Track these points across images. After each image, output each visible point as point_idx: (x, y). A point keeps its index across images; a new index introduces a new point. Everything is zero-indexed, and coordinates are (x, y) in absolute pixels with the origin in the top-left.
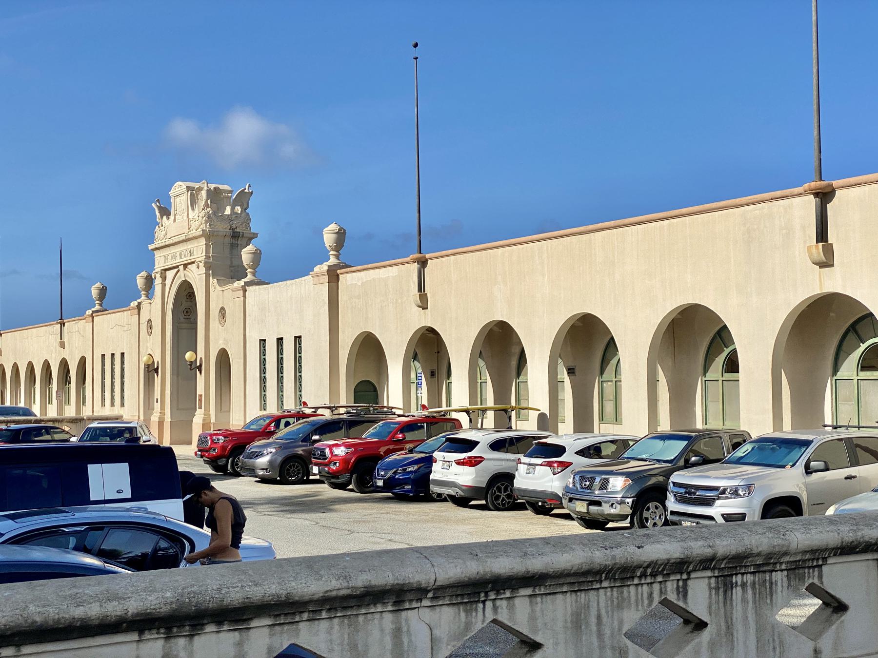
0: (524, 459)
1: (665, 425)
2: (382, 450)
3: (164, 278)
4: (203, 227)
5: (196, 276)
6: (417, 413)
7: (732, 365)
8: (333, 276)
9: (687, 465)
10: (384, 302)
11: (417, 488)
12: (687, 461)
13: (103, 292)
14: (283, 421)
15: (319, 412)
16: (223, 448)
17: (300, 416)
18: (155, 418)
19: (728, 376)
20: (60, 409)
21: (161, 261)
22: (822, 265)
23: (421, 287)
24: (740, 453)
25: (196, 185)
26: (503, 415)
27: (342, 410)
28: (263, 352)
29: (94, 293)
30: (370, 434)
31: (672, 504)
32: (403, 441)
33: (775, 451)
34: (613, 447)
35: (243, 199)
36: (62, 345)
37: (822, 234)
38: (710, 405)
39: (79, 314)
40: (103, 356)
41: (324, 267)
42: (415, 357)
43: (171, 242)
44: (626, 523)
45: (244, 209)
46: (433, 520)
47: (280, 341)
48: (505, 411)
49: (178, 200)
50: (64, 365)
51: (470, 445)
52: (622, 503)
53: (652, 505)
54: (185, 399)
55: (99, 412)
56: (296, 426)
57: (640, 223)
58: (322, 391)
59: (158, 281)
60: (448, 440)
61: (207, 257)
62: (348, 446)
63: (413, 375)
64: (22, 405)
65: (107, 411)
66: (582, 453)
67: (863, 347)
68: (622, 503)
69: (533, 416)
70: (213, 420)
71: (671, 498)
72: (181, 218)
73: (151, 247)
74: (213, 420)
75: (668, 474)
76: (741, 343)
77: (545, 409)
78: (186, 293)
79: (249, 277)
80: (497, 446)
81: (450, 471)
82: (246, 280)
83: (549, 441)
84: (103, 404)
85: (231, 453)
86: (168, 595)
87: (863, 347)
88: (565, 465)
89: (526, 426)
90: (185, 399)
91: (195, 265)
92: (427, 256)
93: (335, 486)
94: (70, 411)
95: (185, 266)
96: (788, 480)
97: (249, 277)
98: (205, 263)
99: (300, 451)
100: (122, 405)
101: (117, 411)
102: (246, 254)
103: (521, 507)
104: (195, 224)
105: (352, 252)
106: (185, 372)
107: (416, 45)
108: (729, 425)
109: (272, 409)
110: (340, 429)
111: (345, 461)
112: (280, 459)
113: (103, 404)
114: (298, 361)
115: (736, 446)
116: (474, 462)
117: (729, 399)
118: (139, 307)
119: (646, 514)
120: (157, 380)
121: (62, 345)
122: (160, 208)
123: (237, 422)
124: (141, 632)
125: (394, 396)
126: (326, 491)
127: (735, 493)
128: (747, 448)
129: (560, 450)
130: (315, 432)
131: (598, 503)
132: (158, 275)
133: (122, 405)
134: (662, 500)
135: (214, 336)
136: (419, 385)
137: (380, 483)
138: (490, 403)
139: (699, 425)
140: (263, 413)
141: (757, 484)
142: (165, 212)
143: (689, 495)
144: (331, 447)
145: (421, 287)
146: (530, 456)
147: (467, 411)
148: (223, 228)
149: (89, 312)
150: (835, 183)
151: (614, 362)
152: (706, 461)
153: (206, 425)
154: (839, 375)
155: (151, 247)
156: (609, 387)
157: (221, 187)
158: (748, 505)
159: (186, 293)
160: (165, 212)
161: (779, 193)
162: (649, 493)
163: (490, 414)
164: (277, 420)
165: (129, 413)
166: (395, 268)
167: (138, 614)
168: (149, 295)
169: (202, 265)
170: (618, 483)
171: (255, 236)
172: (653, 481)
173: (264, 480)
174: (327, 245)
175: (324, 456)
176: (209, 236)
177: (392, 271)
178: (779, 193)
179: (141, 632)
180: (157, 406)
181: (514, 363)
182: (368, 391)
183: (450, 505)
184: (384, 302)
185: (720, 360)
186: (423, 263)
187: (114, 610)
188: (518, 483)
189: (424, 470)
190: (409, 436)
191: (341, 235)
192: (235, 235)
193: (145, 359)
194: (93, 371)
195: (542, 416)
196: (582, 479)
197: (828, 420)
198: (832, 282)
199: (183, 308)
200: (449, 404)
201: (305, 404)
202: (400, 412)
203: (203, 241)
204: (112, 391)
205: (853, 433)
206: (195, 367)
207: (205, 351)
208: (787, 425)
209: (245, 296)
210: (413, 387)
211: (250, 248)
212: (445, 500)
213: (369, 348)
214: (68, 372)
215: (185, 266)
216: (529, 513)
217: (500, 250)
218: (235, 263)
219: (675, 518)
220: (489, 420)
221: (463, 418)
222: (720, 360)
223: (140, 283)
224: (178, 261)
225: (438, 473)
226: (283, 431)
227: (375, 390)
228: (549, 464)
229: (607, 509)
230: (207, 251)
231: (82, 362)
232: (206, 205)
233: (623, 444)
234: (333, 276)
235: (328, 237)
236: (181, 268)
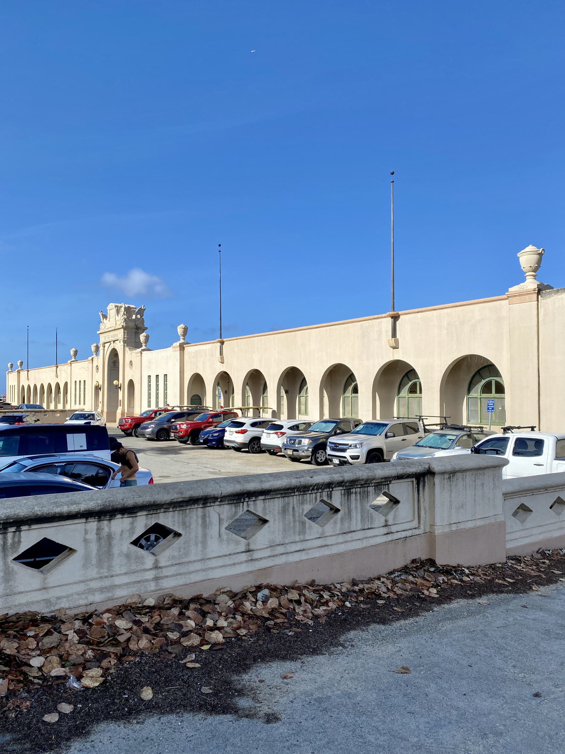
0: (265, 431)
1: (326, 417)
2: (203, 426)
3: (104, 347)
4: (122, 324)
5: (119, 346)
6: (219, 410)
8: (182, 348)
9: (336, 434)
10: (205, 359)
11: (218, 443)
12: (335, 432)
13: (76, 353)
14: (158, 413)
15: (175, 409)
16: (130, 425)
17: (166, 410)
18: (99, 410)
19: (354, 395)
20: (56, 406)
21: (102, 339)
22: (394, 348)
23: (221, 354)
24: (358, 429)
25: (119, 305)
26: (257, 411)
27: (185, 408)
28: (149, 381)
29: (72, 353)
30: (197, 419)
31: (329, 451)
32: (210, 422)
33: (372, 428)
34: (304, 426)
35: (141, 312)
36: (57, 376)
37: (394, 335)
38: (346, 407)
39: (64, 362)
40: (76, 382)
41: (178, 344)
42: (218, 385)
43: (107, 330)
44: (309, 459)
45: (141, 316)
46: (225, 458)
47: (157, 376)
48: (258, 409)
49: (111, 311)
50: (58, 385)
51: (241, 424)
52: (307, 450)
53: (320, 451)
54: (113, 402)
55: (73, 408)
56: (164, 414)
57: (317, 328)
58: (175, 400)
59: (101, 348)
60: (232, 422)
61: (124, 338)
62: (187, 424)
63: (217, 393)
64: (38, 403)
65: (77, 407)
66: (290, 428)
67: (410, 383)
68: (307, 450)
69: (270, 411)
70: (126, 412)
71: (328, 448)
72: (112, 320)
73: (98, 332)
74: (126, 412)
75: (327, 438)
77: (275, 408)
78: (114, 354)
79: (144, 347)
80: (254, 425)
81: (232, 436)
82: (142, 348)
83: (276, 423)
84: (75, 404)
85: (134, 427)
86: (99, 502)
87: (410, 383)
88: (283, 434)
89: (266, 416)
90: (113, 402)
91: (118, 341)
92: (224, 340)
93: (181, 442)
94: (60, 407)
95: (114, 341)
96: (377, 441)
97: (144, 347)
98: (123, 341)
99: (165, 426)
100: (84, 404)
101: (82, 407)
102: (142, 337)
103: (264, 452)
104: (118, 323)
105: (190, 337)
106: (114, 390)
107: (220, 245)
108: (354, 416)
109: (153, 407)
110: (184, 416)
111: (186, 431)
112: (156, 430)
113: (75, 404)
114: (165, 386)
115: (356, 426)
116: (243, 432)
117: (354, 405)
118: (92, 359)
119: (317, 455)
120: (101, 393)
121: (57, 376)
122: (102, 315)
123: (137, 413)
124: (87, 519)
125: (208, 402)
126: (177, 443)
127: (356, 447)
128: (361, 427)
129: (281, 427)
130: (173, 418)
131: (297, 451)
132: (101, 346)
133: (84, 404)
134: (325, 449)
135: (127, 373)
136: (220, 397)
137: (202, 441)
138: (251, 405)
139: (341, 417)
140: (149, 409)
141: (365, 443)
142: (105, 317)
143: (336, 447)
144: (180, 424)
145: (221, 354)
146: (268, 429)
147: (241, 409)
148: (132, 324)
149: (69, 362)
150: (400, 313)
151: (305, 388)
152: (344, 432)
153: (123, 414)
154: (400, 395)
155: (98, 332)
156: (303, 399)
157: (131, 306)
158: (361, 452)
159: (114, 354)
160: (105, 317)
161: (376, 316)
162: (319, 446)
163: (251, 410)
164: (156, 412)
165: (88, 408)
166: (210, 345)
167: (85, 511)
168: (97, 355)
169: (121, 341)
170: (306, 442)
171: (147, 328)
172: (321, 441)
173: (149, 439)
174: (179, 334)
175: (176, 429)
176: (124, 328)
177: (209, 346)
178: (376, 316)
179: (87, 519)
180: (100, 405)
181: (262, 388)
182: (197, 399)
183: (232, 451)
184: (205, 359)
186: (222, 343)
187: (74, 509)
188: (263, 441)
189: (221, 435)
190: (215, 420)
191: (186, 330)
192: (137, 328)
193: (95, 383)
194: (71, 388)
195: (274, 412)
196: (290, 440)
197: (395, 415)
199: (113, 360)
200: (233, 406)
201: (168, 405)
202: (211, 409)
203: (122, 330)
204: (80, 397)
205: (405, 421)
206: (118, 387)
207: (123, 380)
208: (378, 417)
209: (141, 356)
210: (217, 398)
211: (144, 334)
212: (230, 449)
213: (197, 379)
214: (59, 388)
215: (114, 341)
216: (267, 454)
217: (256, 338)
218: (137, 340)
219: (330, 457)
220: (251, 413)
221: (239, 412)
222: (351, 388)
223: (93, 348)
224: (111, 339)
225: (227, 437)
226: (158, 417)
227: (200, 399)
228: (276, 433)
229: (301, 453)
230: (124, 335)
231: (66, 384)
232: (124, 314)
233: (308, 425)
234: (182, 348)
235: (180, 330)
236: (112, 342)
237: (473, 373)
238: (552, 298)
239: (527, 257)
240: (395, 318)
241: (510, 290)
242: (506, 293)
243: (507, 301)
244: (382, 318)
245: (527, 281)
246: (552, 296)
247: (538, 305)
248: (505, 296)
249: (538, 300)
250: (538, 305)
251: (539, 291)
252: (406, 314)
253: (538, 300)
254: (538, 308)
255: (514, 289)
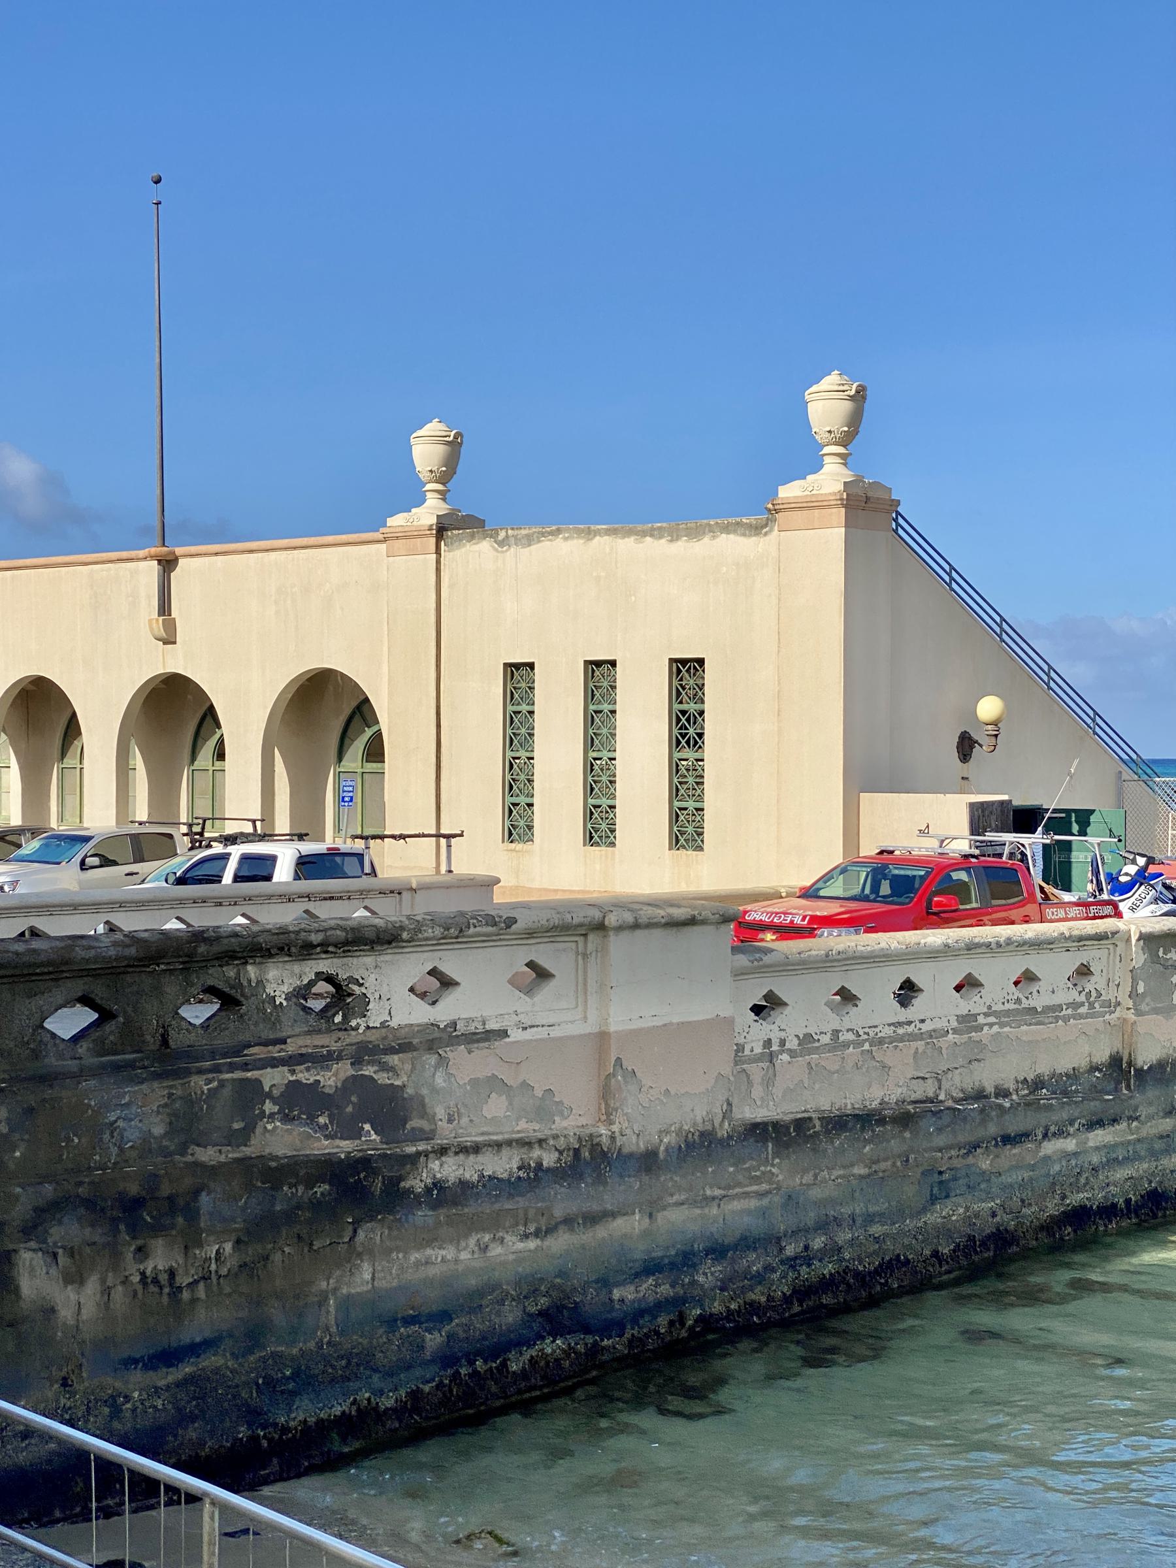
7: (375, 751)
37: (164, 607)
76: (228, 728)
150: (179, 551)
154: (198, 764)
161: (125, 554)
178: (125, 554)
185: (358, 747)
198: (175, 662)
222: (212, 743)
237: (347, 711)
238: (463, 550)
239: (425, 452)
240: (168, 564)
241: (390, 522)
242: (382, 530)
243: (384, 546)
244: (139, 559)
245: (429, 503)
246: (464, 545)
247: (438, 562)
248: (381, 537)
249: (438, 551)
250: (438, 562)
251: (441, 530)
252: (192, 556)
253: (438, 551)
254: (438, 570)
255: (397, 521)
